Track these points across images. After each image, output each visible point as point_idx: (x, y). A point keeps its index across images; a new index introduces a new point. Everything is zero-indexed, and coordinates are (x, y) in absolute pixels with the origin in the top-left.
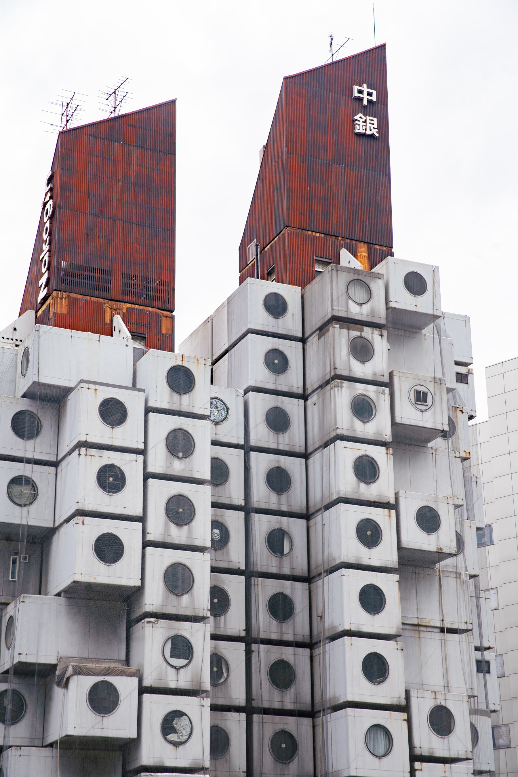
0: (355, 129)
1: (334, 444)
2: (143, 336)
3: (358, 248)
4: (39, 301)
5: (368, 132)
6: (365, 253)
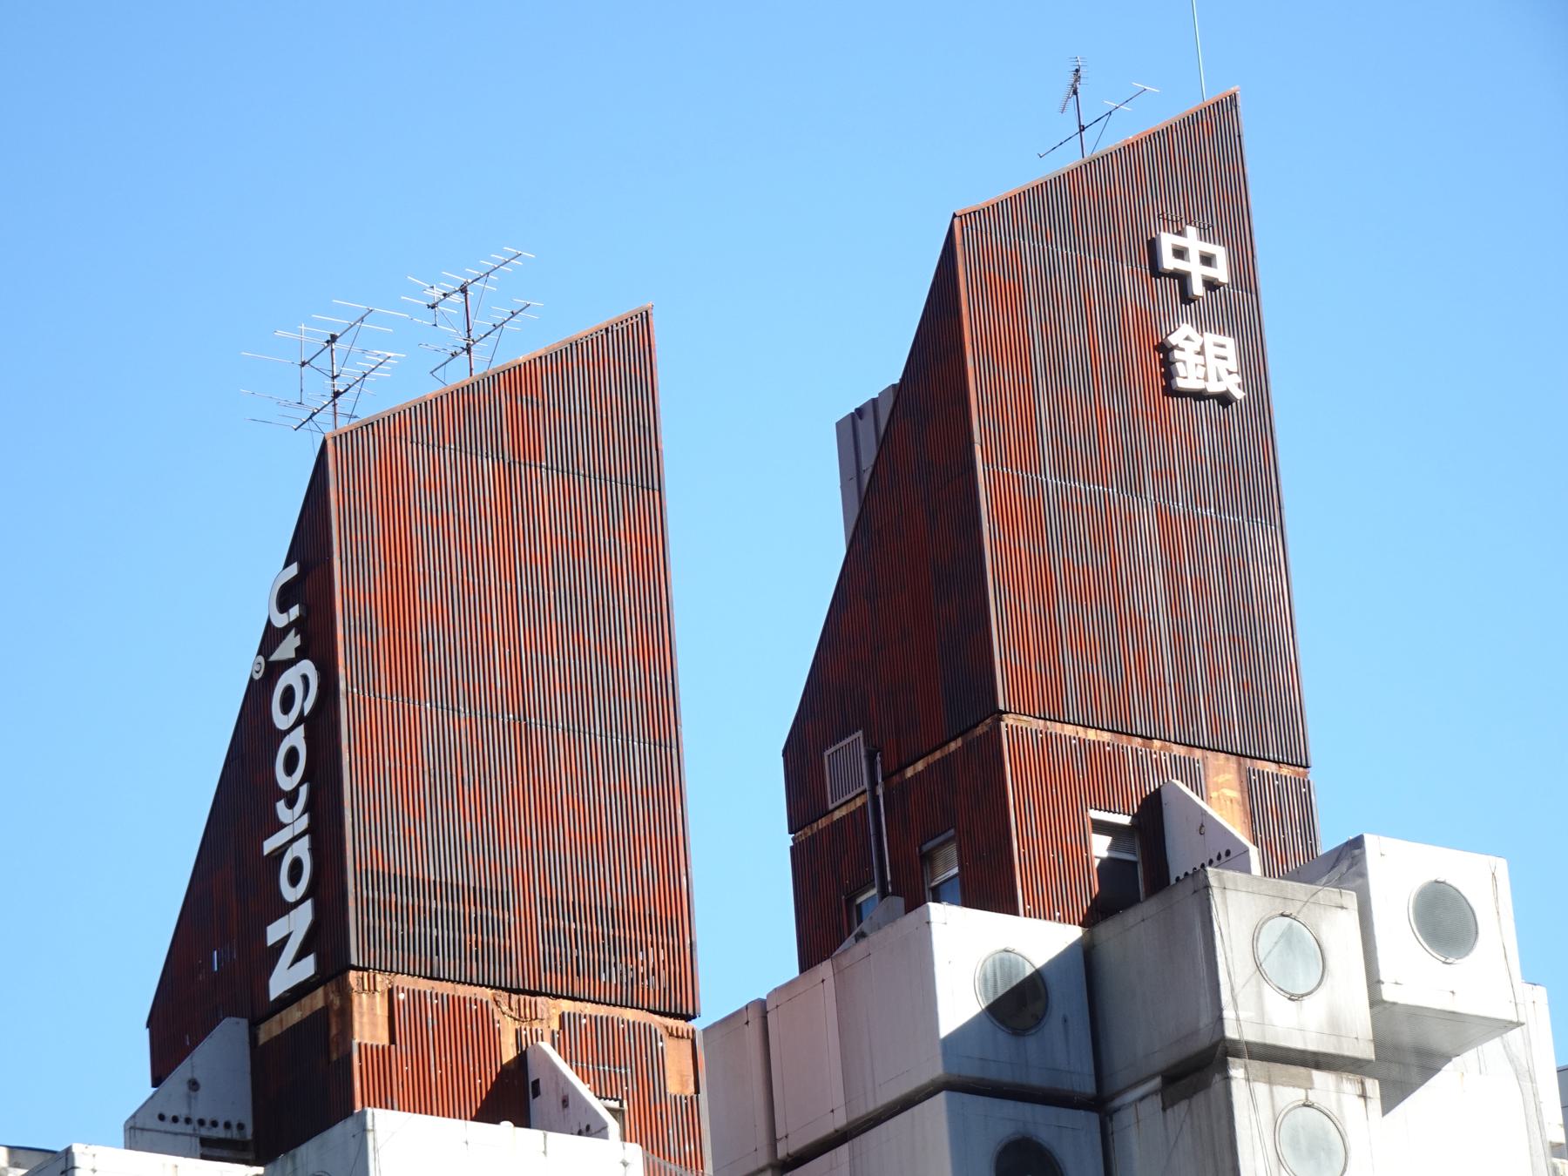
3: (1211, 772)
4: (275, 992)
5: (1214, 387)
6: (1232, 789)
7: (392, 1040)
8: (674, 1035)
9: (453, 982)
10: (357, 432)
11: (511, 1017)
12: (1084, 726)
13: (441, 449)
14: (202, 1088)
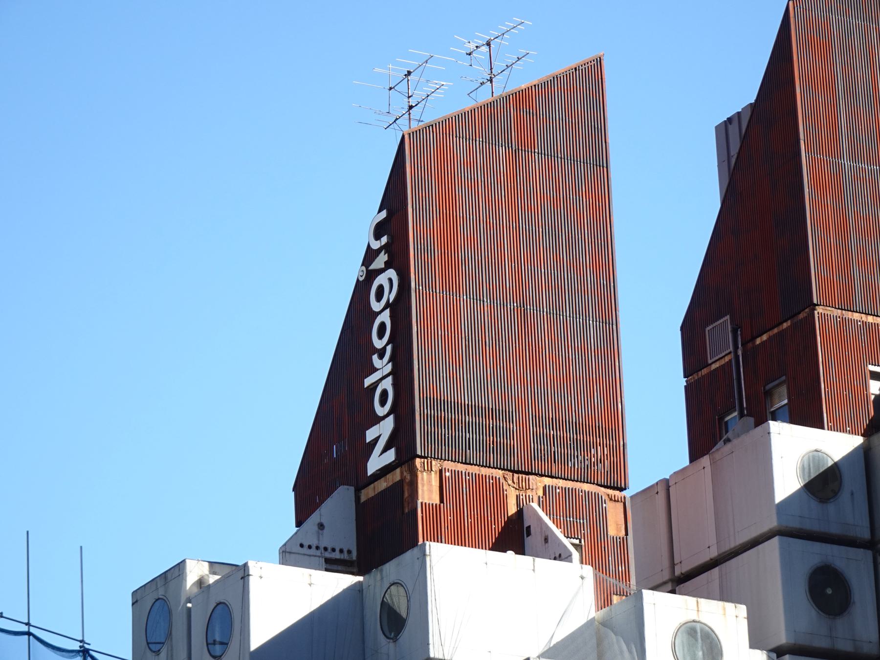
7: (442, 501)
8: (612, 499)
9: (478, 466)
10: (423, 130)
11: (514, 487)
12: (865, 314)
13: (474, 141)
14: (326, 529)
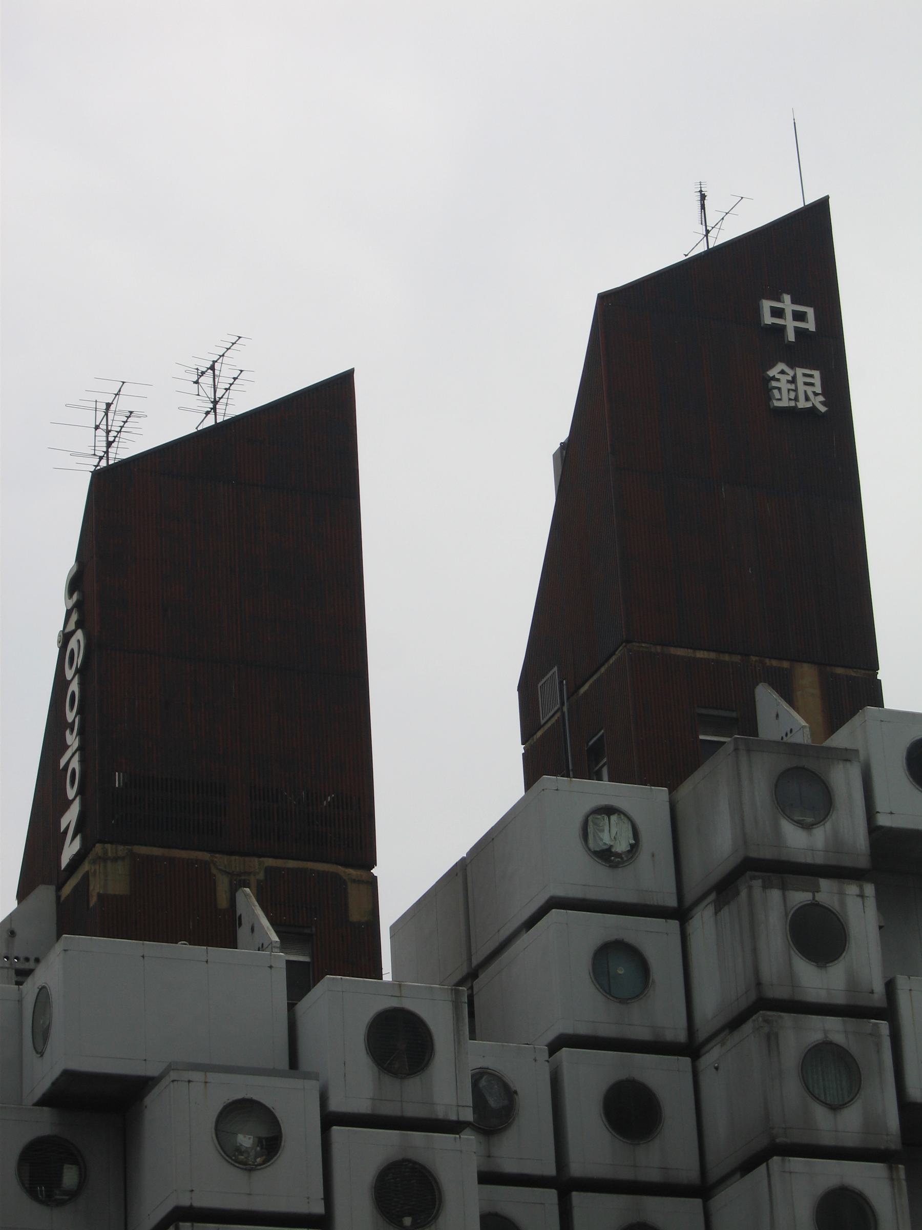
0: (769, 398)
1: (767, 1165)
2: (307, 931)
5: (802, 404)
